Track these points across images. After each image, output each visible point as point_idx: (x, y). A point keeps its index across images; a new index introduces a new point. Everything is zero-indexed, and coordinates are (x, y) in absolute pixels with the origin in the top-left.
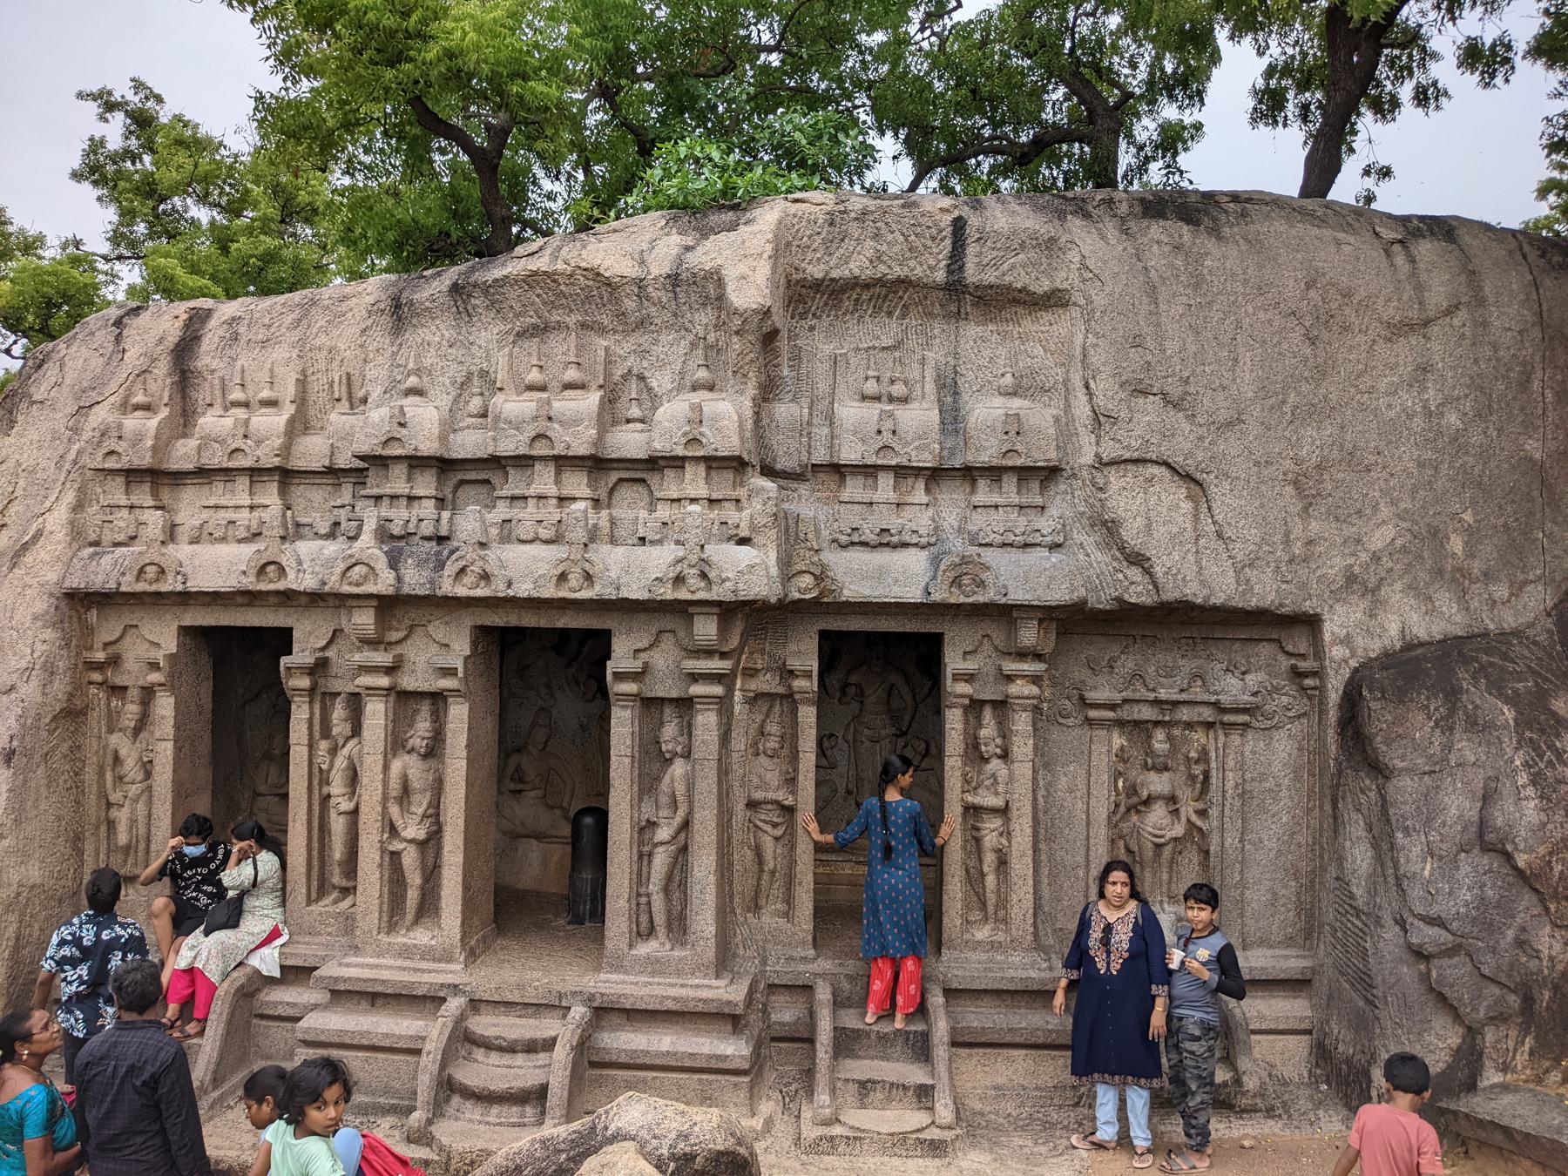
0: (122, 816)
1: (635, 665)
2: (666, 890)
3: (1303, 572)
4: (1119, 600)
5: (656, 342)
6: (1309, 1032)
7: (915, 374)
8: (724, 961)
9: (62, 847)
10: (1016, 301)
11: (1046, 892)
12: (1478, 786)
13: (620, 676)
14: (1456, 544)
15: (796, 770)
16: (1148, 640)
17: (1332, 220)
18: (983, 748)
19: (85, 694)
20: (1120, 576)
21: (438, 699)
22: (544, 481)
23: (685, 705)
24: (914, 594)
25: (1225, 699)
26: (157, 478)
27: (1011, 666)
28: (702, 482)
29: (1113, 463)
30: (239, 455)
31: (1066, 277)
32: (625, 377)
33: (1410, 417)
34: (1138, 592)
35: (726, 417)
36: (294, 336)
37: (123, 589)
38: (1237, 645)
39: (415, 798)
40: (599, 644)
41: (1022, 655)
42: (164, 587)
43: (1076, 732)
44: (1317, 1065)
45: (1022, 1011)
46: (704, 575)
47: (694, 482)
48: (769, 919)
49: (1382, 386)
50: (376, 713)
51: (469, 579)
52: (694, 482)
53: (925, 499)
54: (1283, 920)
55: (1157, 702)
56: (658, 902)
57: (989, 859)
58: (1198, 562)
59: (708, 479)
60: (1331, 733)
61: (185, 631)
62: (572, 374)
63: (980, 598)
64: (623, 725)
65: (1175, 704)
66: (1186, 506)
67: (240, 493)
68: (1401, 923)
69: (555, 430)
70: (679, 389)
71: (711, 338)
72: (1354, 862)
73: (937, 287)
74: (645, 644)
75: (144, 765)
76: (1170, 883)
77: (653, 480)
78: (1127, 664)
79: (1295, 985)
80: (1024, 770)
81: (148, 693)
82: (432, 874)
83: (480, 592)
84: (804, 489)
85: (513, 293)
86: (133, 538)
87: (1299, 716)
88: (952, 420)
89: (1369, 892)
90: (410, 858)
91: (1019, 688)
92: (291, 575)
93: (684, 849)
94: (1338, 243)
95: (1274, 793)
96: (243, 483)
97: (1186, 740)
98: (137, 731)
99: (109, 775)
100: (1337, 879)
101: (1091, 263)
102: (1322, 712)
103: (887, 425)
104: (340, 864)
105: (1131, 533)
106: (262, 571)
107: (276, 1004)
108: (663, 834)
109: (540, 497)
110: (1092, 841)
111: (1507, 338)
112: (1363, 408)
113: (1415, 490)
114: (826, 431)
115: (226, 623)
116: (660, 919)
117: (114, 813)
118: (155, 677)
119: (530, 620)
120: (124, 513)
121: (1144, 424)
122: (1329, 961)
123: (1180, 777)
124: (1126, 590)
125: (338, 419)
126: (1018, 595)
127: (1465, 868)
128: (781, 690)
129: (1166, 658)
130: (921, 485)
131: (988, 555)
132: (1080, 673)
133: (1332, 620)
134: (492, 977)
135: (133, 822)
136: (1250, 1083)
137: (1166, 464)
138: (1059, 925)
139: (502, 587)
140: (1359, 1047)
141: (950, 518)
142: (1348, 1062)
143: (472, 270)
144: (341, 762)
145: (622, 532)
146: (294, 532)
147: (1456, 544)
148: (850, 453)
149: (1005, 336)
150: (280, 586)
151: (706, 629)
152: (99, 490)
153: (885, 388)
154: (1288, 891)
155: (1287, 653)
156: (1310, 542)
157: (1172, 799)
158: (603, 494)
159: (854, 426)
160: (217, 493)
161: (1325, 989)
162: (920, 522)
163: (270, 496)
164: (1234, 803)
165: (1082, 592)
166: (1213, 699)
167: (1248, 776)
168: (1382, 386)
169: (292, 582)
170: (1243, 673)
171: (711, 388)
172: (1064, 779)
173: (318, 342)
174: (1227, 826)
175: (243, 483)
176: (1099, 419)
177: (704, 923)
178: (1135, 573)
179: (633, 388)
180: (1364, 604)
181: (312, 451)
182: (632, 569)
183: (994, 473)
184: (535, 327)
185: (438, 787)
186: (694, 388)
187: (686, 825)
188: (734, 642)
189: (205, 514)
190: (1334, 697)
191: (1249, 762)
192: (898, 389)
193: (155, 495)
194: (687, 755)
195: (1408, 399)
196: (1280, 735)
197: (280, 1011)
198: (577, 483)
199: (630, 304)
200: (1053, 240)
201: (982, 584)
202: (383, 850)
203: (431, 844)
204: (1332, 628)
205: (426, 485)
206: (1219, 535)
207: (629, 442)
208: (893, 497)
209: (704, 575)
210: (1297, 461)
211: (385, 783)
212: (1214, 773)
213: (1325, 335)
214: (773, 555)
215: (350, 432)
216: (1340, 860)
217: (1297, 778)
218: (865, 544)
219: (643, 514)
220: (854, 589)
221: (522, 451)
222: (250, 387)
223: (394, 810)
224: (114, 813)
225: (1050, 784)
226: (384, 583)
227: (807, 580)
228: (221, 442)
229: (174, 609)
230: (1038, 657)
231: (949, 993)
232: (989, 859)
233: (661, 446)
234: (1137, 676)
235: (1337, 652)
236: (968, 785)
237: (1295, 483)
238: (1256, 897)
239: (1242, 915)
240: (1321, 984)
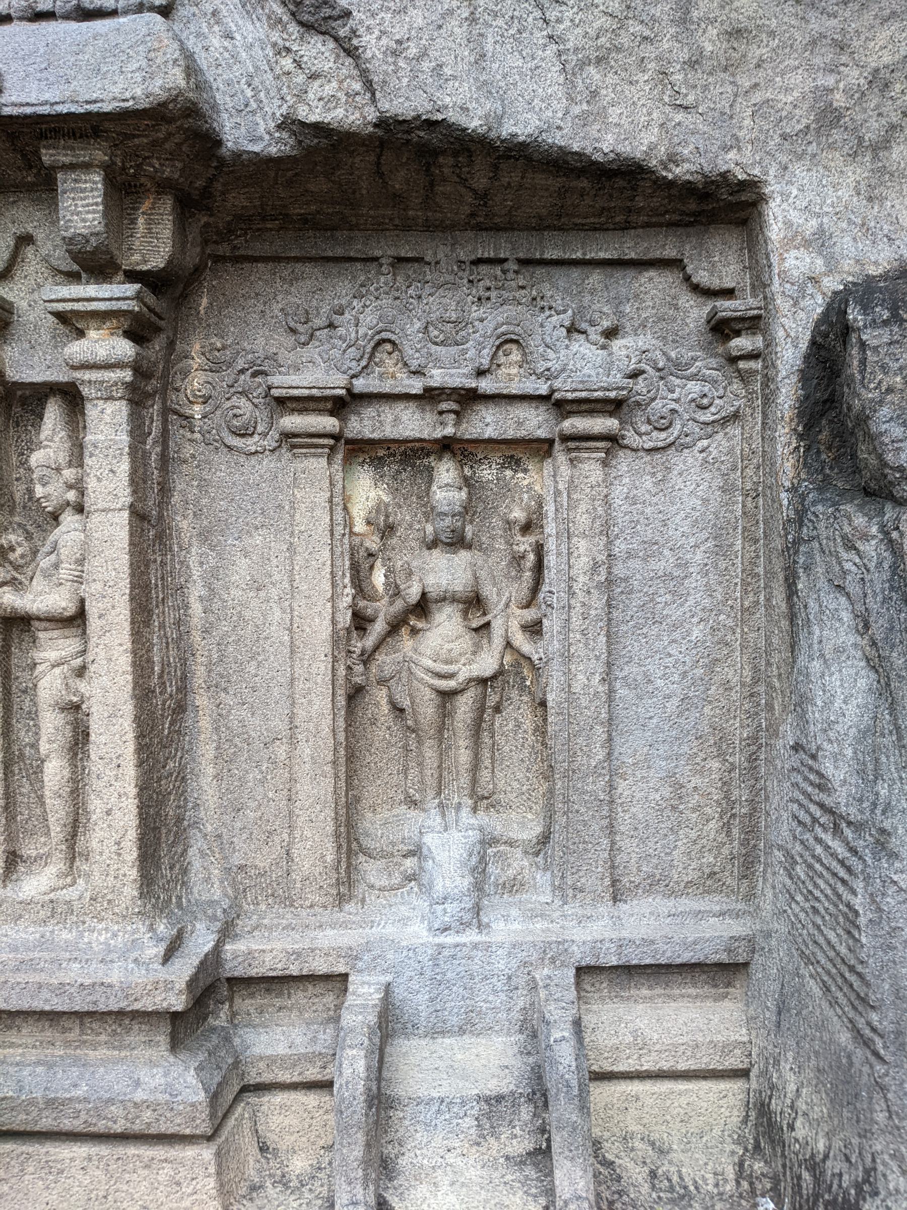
3: (721, 91)
4: (289, 124)
6: (743, 1074)
16: (411, 269)
18: (39, 491)
20: (287, 63)
25: (566, 388)
38: (595, 278)
43: (268, 463)
44: (757, 1147)
45: (102, 1052)
54: (697, 839)
55: (430, 396)
58: (475, 41)
60: (784, 435)
72: (827, 705)
76: (475, 767)
78: (365, 318)
79: (721, 973)
80: (111, 530)
87: (725, 421)
89: (861, 772)
95: (674, 582)
97: (507, 489)
100: (797, 747)
102: (768, 400)
110: (300, 685)
122: (781, 927)
123: (499, 562)
124: (302, 94)
129: (440, 304)
133: (785, 196)
138: (237, 860)
140: (838, 1144)
142: (815, 1165)
154: (705, 781)
155: (696, 289)
156: (736, 33)
157: (474, 602)
161: (776, 986)
166: (543, 390)
167: (620, 547)
170: (611, 333)
172: (244, 562)
174: (578, 649)
180: (856, 174)
191: (621, 519)
212: (551, 545)
217: (721, 550)
225: (214, 573)
238: (641, 795)
239: (611, 829)
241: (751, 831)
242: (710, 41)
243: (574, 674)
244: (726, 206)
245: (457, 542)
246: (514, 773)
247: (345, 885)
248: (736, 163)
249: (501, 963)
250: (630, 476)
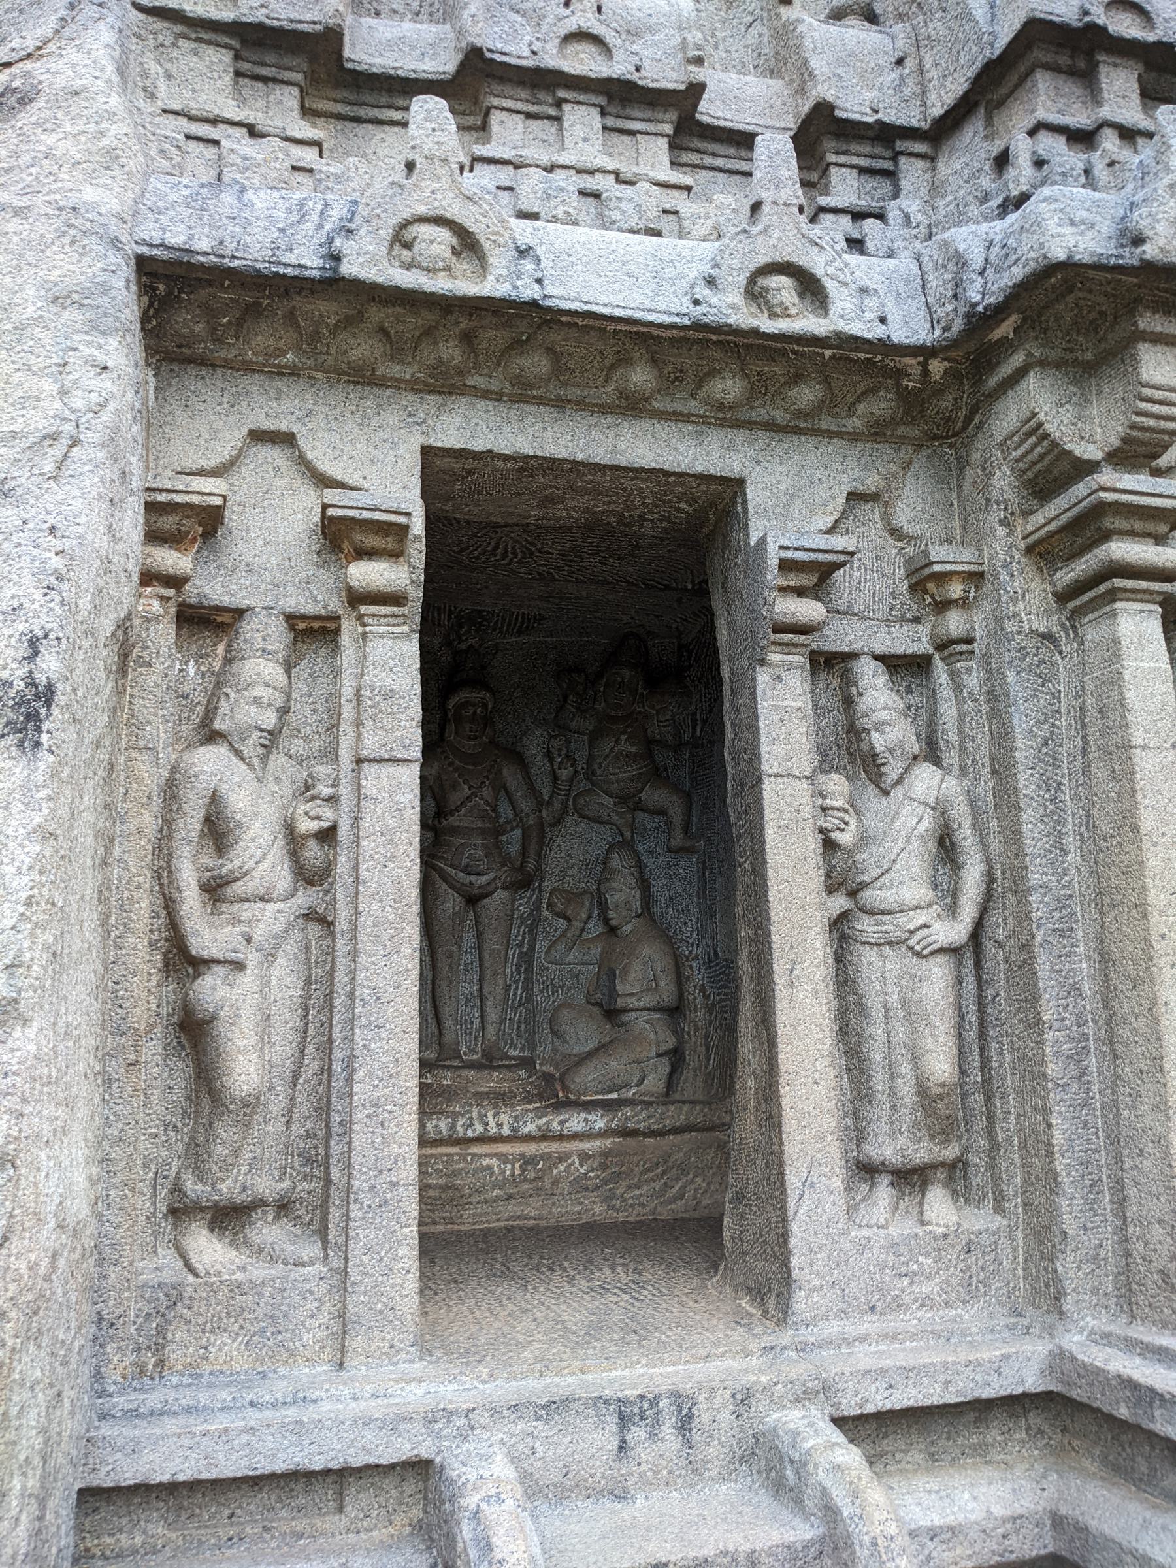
37: (349, 269)
115: (562, 452)
117: (211, 990)
152: (153, 68)
169: (846, 317)
224: (211, 990)
229: (408, 399)
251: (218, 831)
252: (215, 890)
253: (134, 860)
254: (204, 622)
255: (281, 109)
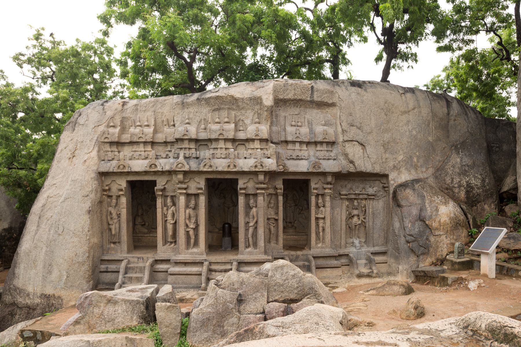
0: (113, 227)
1: (245, 186)
2: (252, 237)
5: (246, 112)
7: (303, 120)
8: (266, 253)
9: (100, 235)
10: (325, 105)
11: (332, 237)
12: (419, 208)
13: (241, 189)
14: (415, 160)
15: (278, 211)
17: (390, 88)
19: (104, 196)
21: (197, 195)
22: (221, 144)
23: (255, 195)
24: (305, 170)
26: (119, 144)
27: (326, 186)
28: (259, 145)
29: (347, 141)
30: (141, 138)
31: (335, 100)
32: (239, 121)
33: (406, 132)
34: (352, 170)
35: (264, 130)
36: (153, 109)
39: (192, 219)
40: (236, 181)
41: (328, 183)
42: (126, 170)
46: (261, 165)
47: (257, 144)
48: (273, 244)
49: (400, 125)
50: (182, 200)
51: (207, 167)
52: (257, 144)
53: (306, 149)
55: (355, 194)
56: (250, 239)
57: (321, 229)
58: (364, 163)
59: (260, 144)
61: (128, 182)
62: (226, 120)
63: (320, 171)
64: (241, 200)
65: (359, 194)
66: (362, 151)
67: (141, 148)
68: (405, 236)
69: (224, 133)
70: (252, 123)
71: (259, 112)
73: (308, 101)
74: (246, 181)
75: (118, 215)
77: (247, 144)
78: (349, 186)
80: (328, 209)
81: (118, 197)
82: (197, 236)
83: (209, 170)
84: (279, 146)
85: (212, 101)
86: (113, 159)
88: (311, 131)
90: (191, 233)
91: (327, 191)
92: (159, 167)
93: (256, 228)
94: (391, 93)
96: (142, 145)
97: (361, 203)
98: (115, 206)
99: (109, 218)
101: (341, 97)
103: (298, 132)
104: (171, 236)
105: (350, 156)
106: (151, 166)
107: (158, 268)
108: (251, 224)
109: (221, 148)
111: (425, 115)
112: (396, 130)
113: (407, 147)
114: (284, 133)
116: (251, 243)
117: (111, 226)
118: (121, 193)
119: (219, 176)
120: (110, 153)
121: (353, 132)
125: (167, 130)
126: (328, 170)
127: (417, 225)
128: (274, 193)
129: (357, 184)
130: (305, 146)
131: (321, 161)
132: (339, 188)
134: (214, 258)
135: (115, 229)
136: (375, 271)
137: (357, 142)
139: (215, 168)
141: (312, 153)
143: (201, 95)
144: (170, 212)
145: (240, 156)
146: (157, 157)
147: (415, 160)
148: (290, 138)
149: (322, 112)
150: (156, 170)
151: (261, 177)
153: (297, 124)
157: (358, 216)
158: (235, 147)
159: (291, 133)
160: (135, 148)
162: (306, 154)
163: (149, 148)
164: (371, 215)
165: (341, 169)
168: (400, 125)
169: (159, 169)
171: (259, 123)
173: (159, 111)
175: (142, 145)
176: (343, 131)
177: (261, 243)
178: (351, 165)
179: (241, 123)
181: (160, 137)
182: (246, 164)
183: (321, 143)
184: (217, 109)
185: (197, 216)
186: (255, 123)
187: (256, 222)
188: (267, 181)
189: (132, 153)
190: (391, 192)
192: (299, 124)
193: (117, 148)
194: (256, 207)
195: (405, 128)
196: (381, 201)
197: (159, 270)
198: (229, 145)
199: (240, 104)
200: (332, 91)
201: (320, 168)
202: (185, 231)
203: (196, 229)
204: (391, 177)
205: (193, 145)
206: (368, 157)
207: (241, 135)
208: (299, 148)
209: (261, 165)
210: (384, 141)
211: (185, 215)
213: (389, 114)
214: (275, 161)
215: (168, 133)
216: (393, 226)
217: (384, 210)
218: (293, 159)
219: (245, 152)
220: (292, 169)
221: (216, 137)
222: (142, 122)
223: (187, 222)
224: (111, 226)
226: (186, 168)
227: (281, 167)
228: (136, 135)
230: (331, 184)
231: (314, 258)
232: (321, 229)
233: (249, 136)
234: (351, 188)
235: (392, 182)
236: (317, 213)
237: (383, 146)
238: (376, 236)
240: (389, 253)
241: (387, 239)
242: (384, 160)
243: (369, 223)
244: (386, 176)
245: (357, 209)
246: (362, 234)
247: (346, 247)
248: (386, 173)
249: (364, 253)
250: (375, 203)
251: (111, 213)
252: (111, 218)
253: (104, 217)
254: (110, 197)
255: (114, 148)
